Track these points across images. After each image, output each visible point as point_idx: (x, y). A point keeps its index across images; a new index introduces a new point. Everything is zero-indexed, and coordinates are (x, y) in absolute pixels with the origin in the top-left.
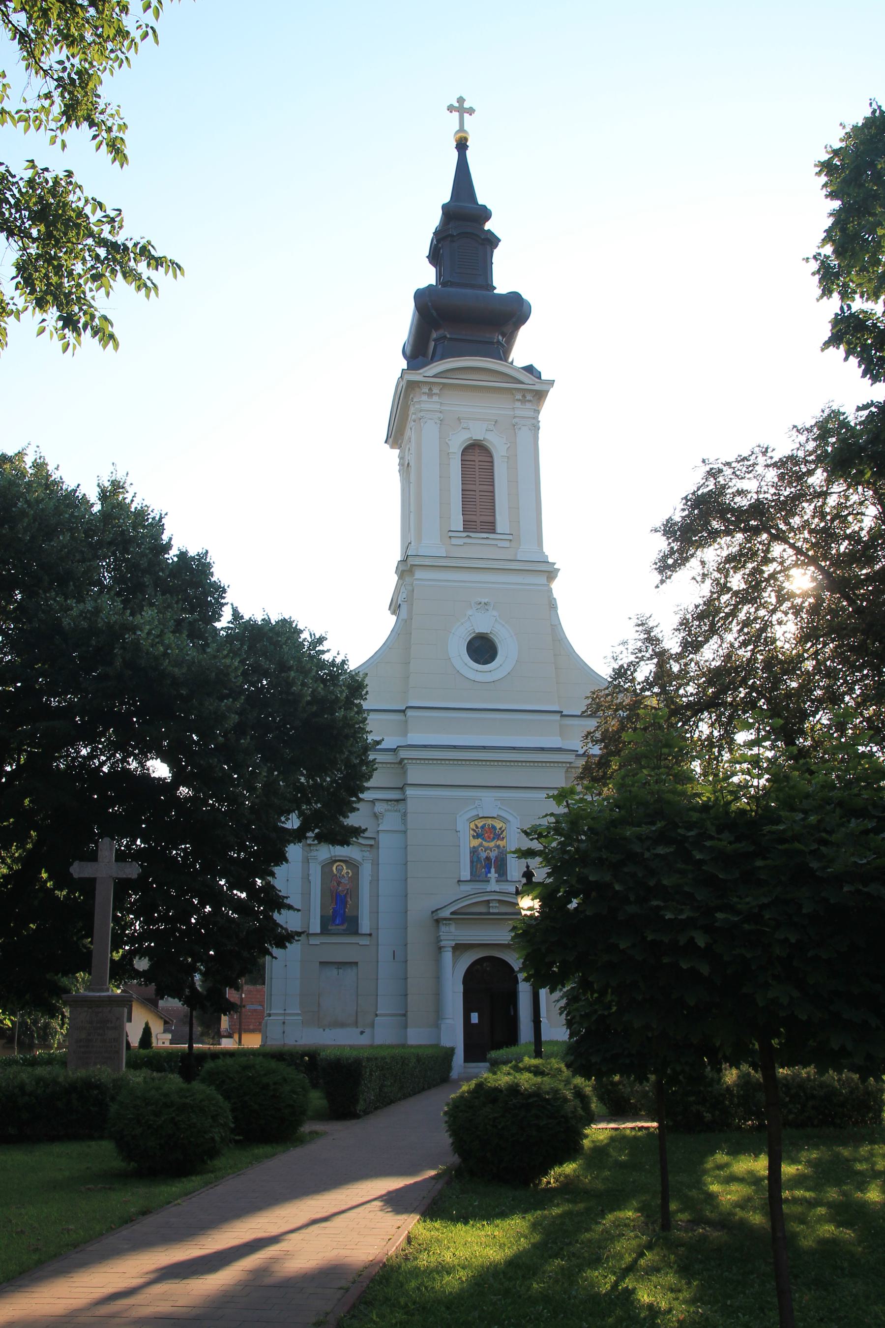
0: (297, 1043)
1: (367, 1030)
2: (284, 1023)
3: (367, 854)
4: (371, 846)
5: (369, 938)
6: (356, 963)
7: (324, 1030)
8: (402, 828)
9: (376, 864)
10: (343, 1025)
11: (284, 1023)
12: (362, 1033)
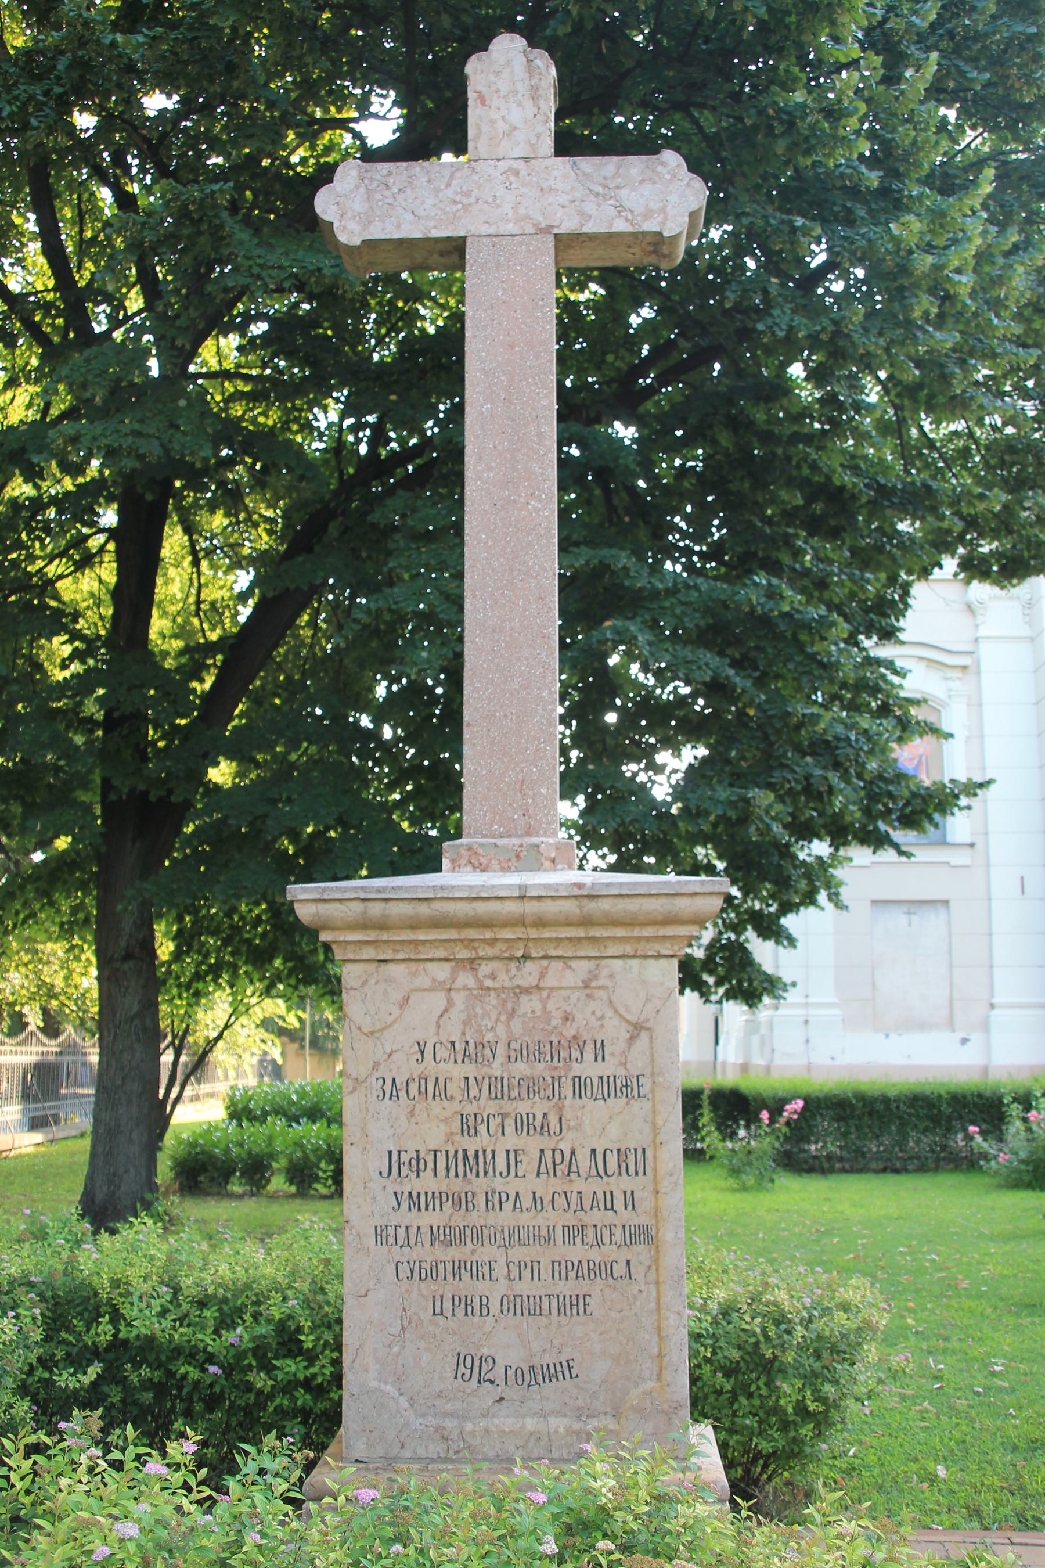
0: (837, 1063)
1: (976, 1038)
2: (806, 1022)
3: (956, 685)
4: (964, 668)
5: (968, 851)
6: (946, 902)
7: (887, 1036)
8: (1026, 632)
9: (976, 704)
10: (922, 1026)
11: (806, 1022)
12: (964, 1041)
